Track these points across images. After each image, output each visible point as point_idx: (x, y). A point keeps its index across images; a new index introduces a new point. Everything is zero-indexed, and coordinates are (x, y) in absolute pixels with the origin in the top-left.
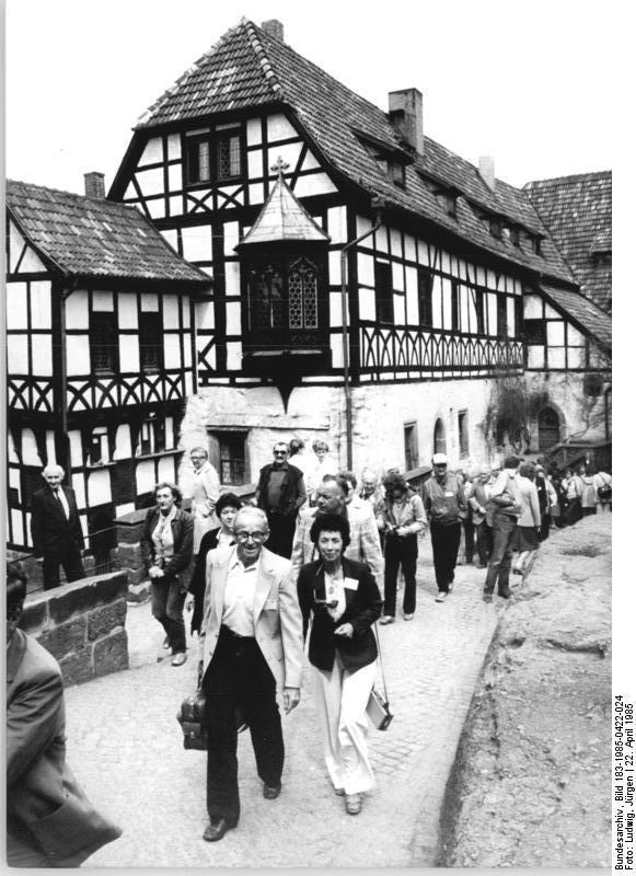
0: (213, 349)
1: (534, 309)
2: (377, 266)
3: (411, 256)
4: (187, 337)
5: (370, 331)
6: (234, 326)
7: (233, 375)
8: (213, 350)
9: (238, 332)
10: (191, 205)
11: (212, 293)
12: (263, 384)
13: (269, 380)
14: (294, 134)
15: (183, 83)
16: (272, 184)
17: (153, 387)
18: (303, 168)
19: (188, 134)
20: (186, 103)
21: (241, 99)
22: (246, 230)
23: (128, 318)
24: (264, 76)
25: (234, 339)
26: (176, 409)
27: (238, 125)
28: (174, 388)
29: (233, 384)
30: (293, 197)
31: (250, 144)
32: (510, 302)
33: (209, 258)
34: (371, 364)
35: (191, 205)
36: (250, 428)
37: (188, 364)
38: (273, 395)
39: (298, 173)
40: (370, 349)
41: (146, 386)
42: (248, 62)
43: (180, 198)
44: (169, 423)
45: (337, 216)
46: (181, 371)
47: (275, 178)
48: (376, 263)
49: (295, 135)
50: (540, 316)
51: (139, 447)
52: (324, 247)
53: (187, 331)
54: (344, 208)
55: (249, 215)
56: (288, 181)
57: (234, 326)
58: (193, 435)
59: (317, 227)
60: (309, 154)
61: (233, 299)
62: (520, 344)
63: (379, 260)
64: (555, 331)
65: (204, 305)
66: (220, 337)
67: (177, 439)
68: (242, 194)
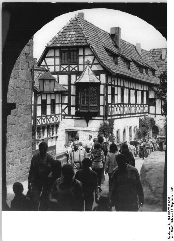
0: (67, 108)
2: (112, 88)
4: (60, 105)
5: (110, 106)
6: (73, 102)
7: (73, 116)
12: (81, 119)
13: (83, 118)
15: (60, 34)
18: (94, 63)
20: (61, 41)
22: (78, 77)
23: (49, 102)
24: (84, 36)
26: (57, 125)
28: (57, 119)
30: (91, 70)
33: (67, 83)
34: (110, 114)
36: (78, 130)
37: (60, 113)
38: (84, 122)
39: (92, 64)
40: (110, 110)
41: (52, 119)
42: (79, 31)
43: (59, 67)
44: (55, 128)
45: (103, 77)
46: (59, 115)
48: (112, 88)
51: (49, 135)
54: (105, 74)
55: (79, 73)
56: (90, 66)
58: (61, 133)
59: (97, 78)
63: (112, 87)
65: (65, 96)
67: (56, 133)
68: (77, 67)
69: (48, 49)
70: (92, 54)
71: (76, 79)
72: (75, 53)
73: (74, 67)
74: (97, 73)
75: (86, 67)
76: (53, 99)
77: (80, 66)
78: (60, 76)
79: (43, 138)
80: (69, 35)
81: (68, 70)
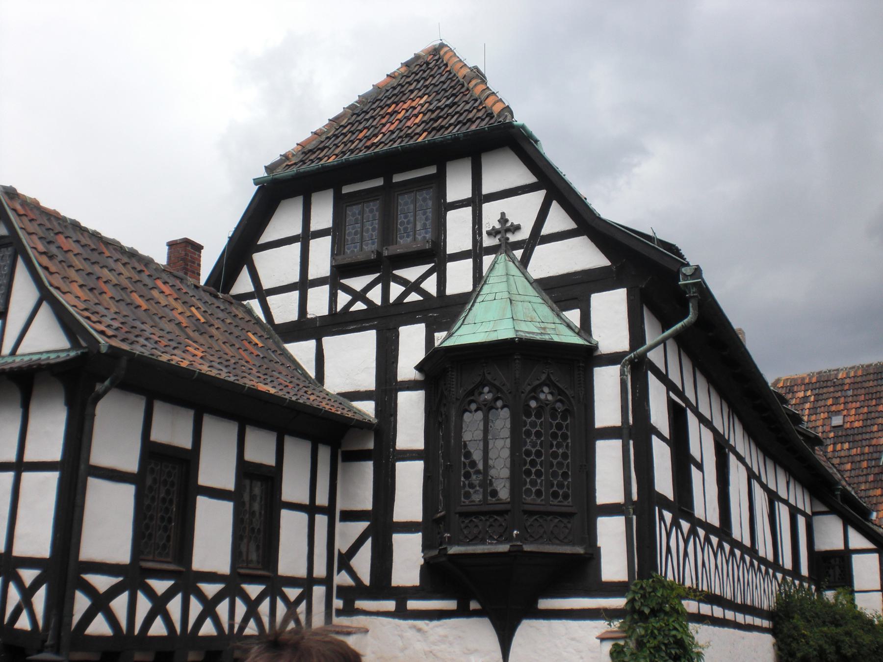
8: (367, 549)
10: (343, 299)
11: (371, 445)
12: (463, 612)
14: (525, 177)
21: (438, 129)
29: (401, 613)
31: (451, 197)
33: (369, 382)
35: (343, 299)
37: (320, 570)
46: (307, 583)
55: (444, 310)
59: (569, 326)
60: (555, 207)
61: (410, 455)
66: (381, 526)
68: (434, 277)
72: (425, 198)
75: (492, 268)
78: (328, 342)
80: (396, 112)
81: (378, 301)
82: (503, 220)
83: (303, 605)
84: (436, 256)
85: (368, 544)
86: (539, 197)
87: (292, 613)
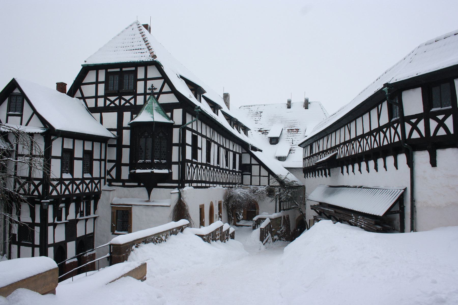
1: (246, 160)
3: (204, 133)
5: (189, 164)
6: (126, 158)
9: (128, 162)
11: (116, 143)
12: (139, 186)
13: (142, 184)
16: (148, 97)
17: (87, 185)
19: (109, 70)
22: (134, 116)
25: (125, 165)
26: (96, 196)
27: (133, 69)
32: (237, 156)
33: (115, 127)
34: (189, 179)
35: (108, 103)
37: (103, 175)
40: (189, 172)
45: (178, 113)
47: (149, 94)
49: (160, 76)
50: (249, 162)
52: (171, 126)
53: (103, 160)
55: (136, 110)
56: (156, 96)
57: (126, 158)
60: (166, 84)
61: (126, 146)
62: (240, 174)
64: (255, 169)
66: (118, 164)
67: (95, 208)
68: (133, 99)
69: (86, 69)
70: (160, 76)
71: (132, 119)
73: (127, 99)
74: (167, 108)
75: (149, 99)
76: (88, 151)
77: (138, 97)
79: (66, 219)
81: (118, 104)
82: (152, 86)
83: (99, 184)
84: (135, 95)
85: (115, 168)
86: (162, 81)
87: (96, 187)
